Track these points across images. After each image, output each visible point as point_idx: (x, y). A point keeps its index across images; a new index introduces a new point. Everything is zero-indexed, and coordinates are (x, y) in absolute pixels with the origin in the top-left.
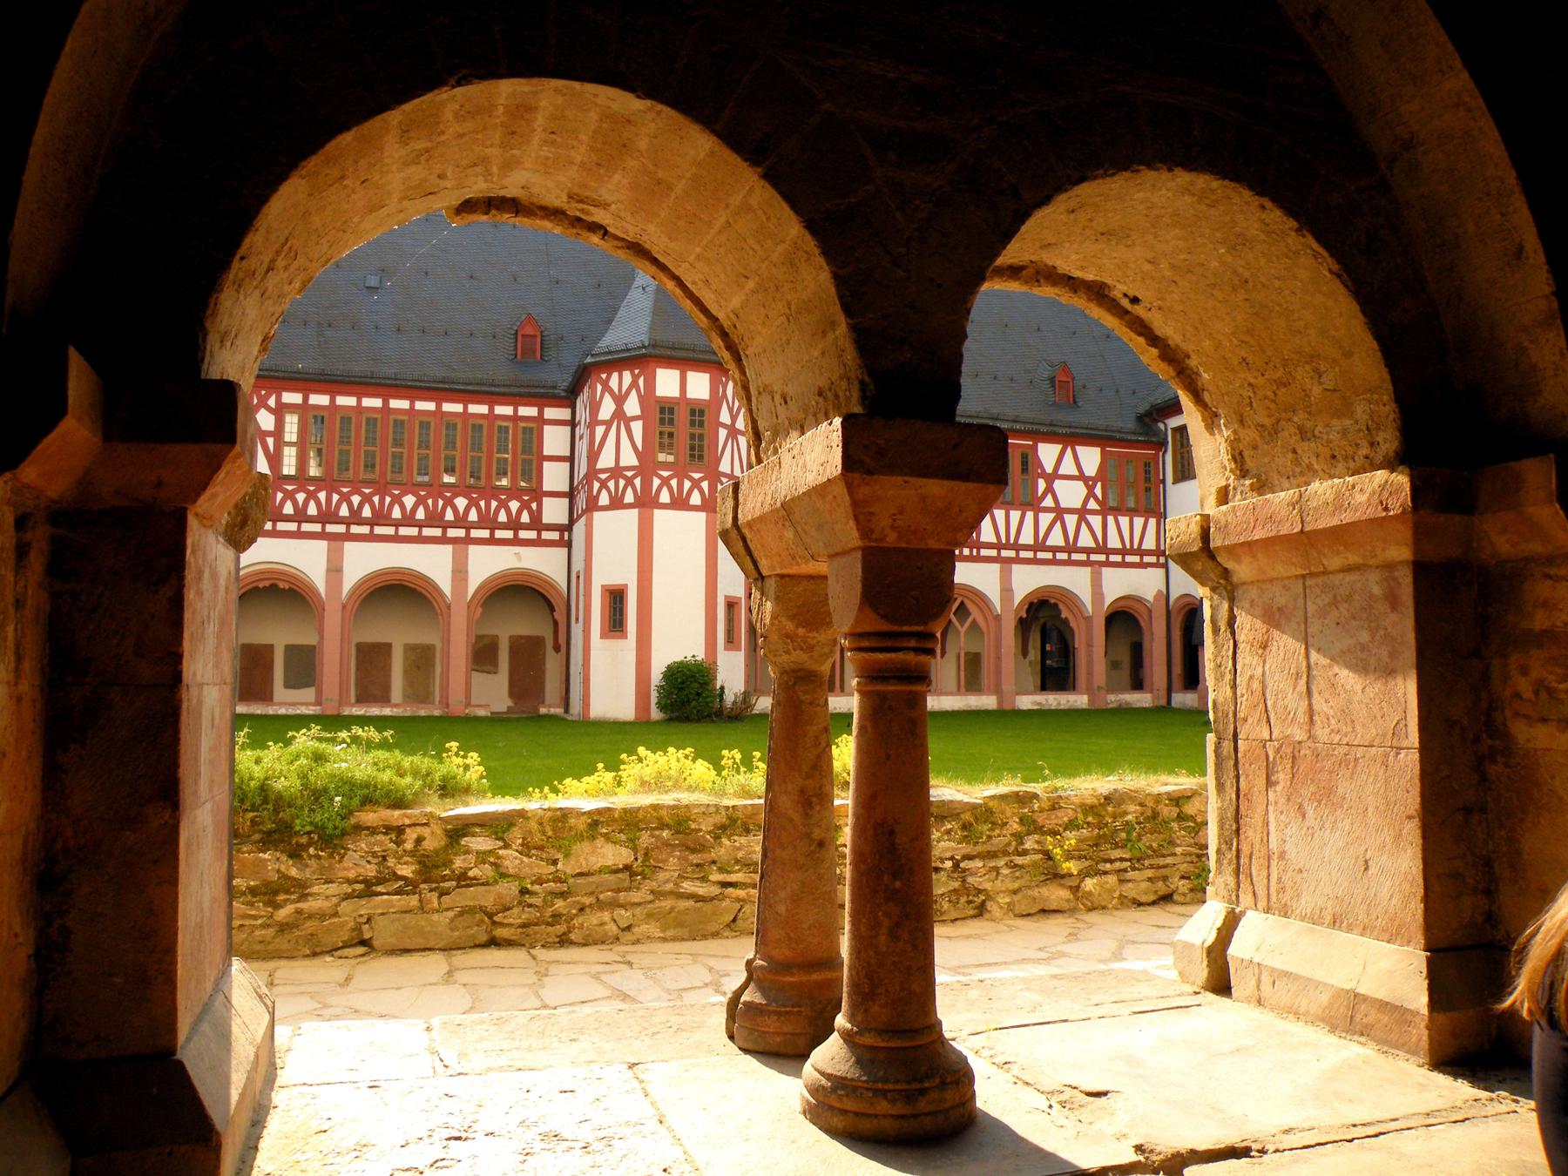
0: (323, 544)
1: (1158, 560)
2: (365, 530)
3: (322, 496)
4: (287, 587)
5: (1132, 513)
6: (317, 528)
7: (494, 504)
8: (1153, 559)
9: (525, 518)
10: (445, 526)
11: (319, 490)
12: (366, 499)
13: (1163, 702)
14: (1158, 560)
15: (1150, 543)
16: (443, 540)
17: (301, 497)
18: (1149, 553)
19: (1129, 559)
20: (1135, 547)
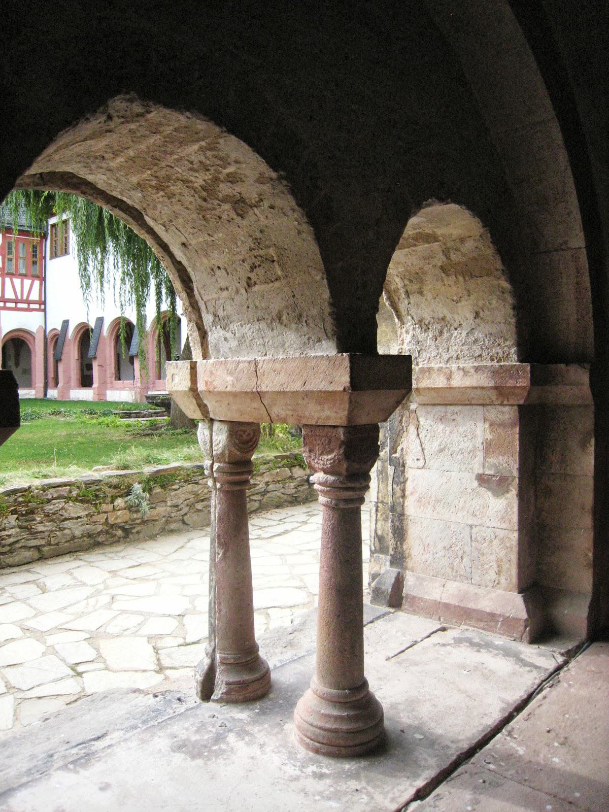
1: (40, 307)
5: (23, 276)
8: (37, 306)
13: (41, 396)
14: (40, 307)
15: (34, 296)
18: (34, 302)
19: (20, 305)
20: (25, 298)
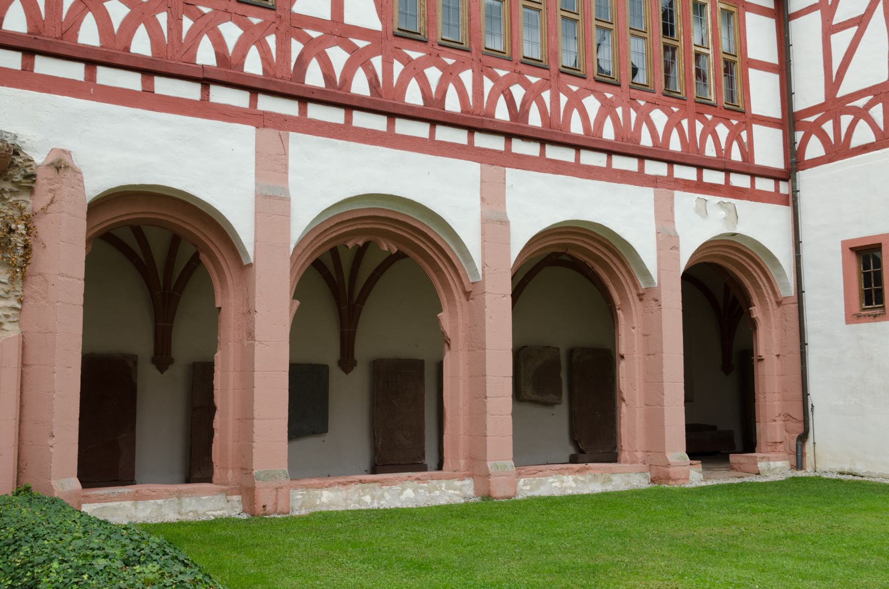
0: (473, 169)
2: (531, 149)
3: (467, 77)
4: (395, 250)
6: (460, 137)
7: (699, 127)
9: (736, 155)
10: (642, 156)
11: (461, 66)
12: (533, 94)
16: (639, 179)
17: (433, 74)
